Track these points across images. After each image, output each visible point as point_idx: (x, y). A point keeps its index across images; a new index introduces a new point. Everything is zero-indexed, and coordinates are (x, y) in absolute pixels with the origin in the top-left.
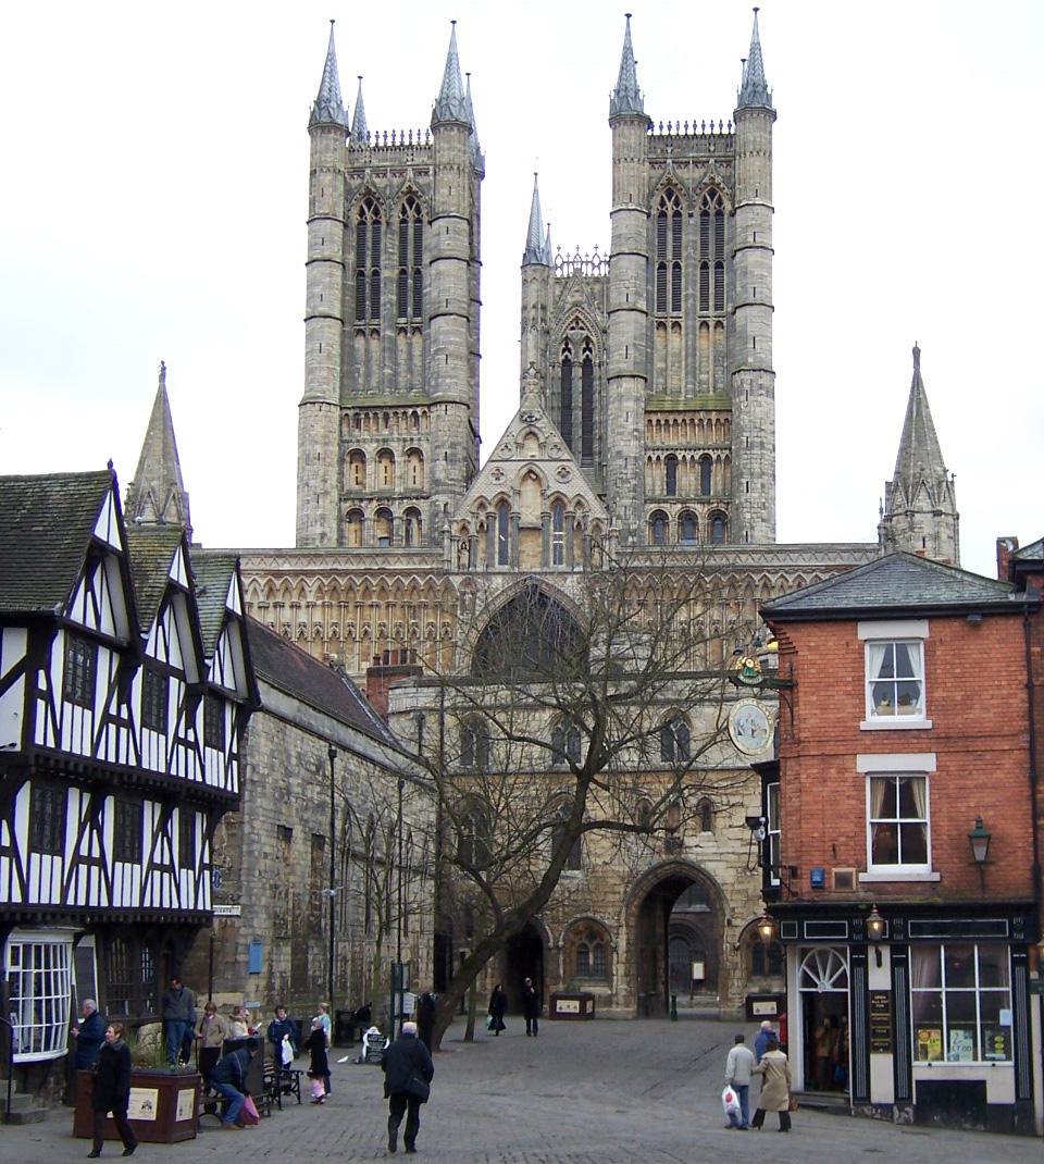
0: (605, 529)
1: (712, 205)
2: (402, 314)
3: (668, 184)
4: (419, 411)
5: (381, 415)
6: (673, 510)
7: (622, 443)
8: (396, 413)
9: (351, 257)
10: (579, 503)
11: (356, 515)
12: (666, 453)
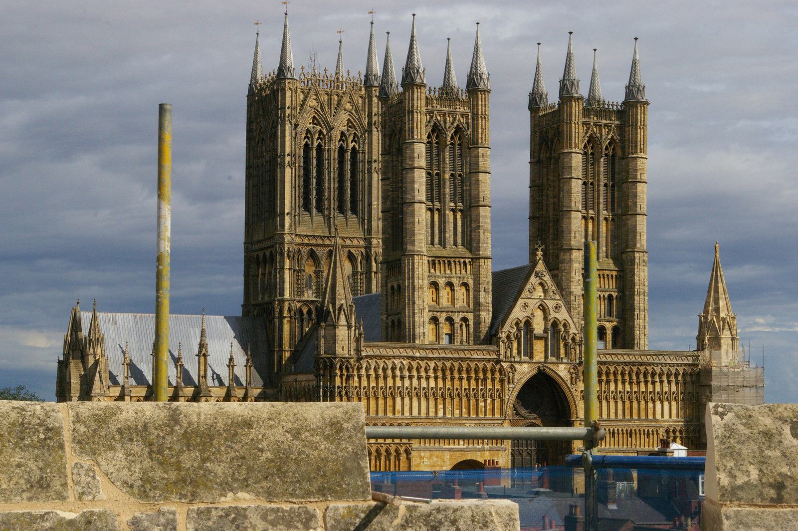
0: (578, 338)
4: (467, 260)
5: (446, 262)
8: (454, 261)
11: (435, 320)
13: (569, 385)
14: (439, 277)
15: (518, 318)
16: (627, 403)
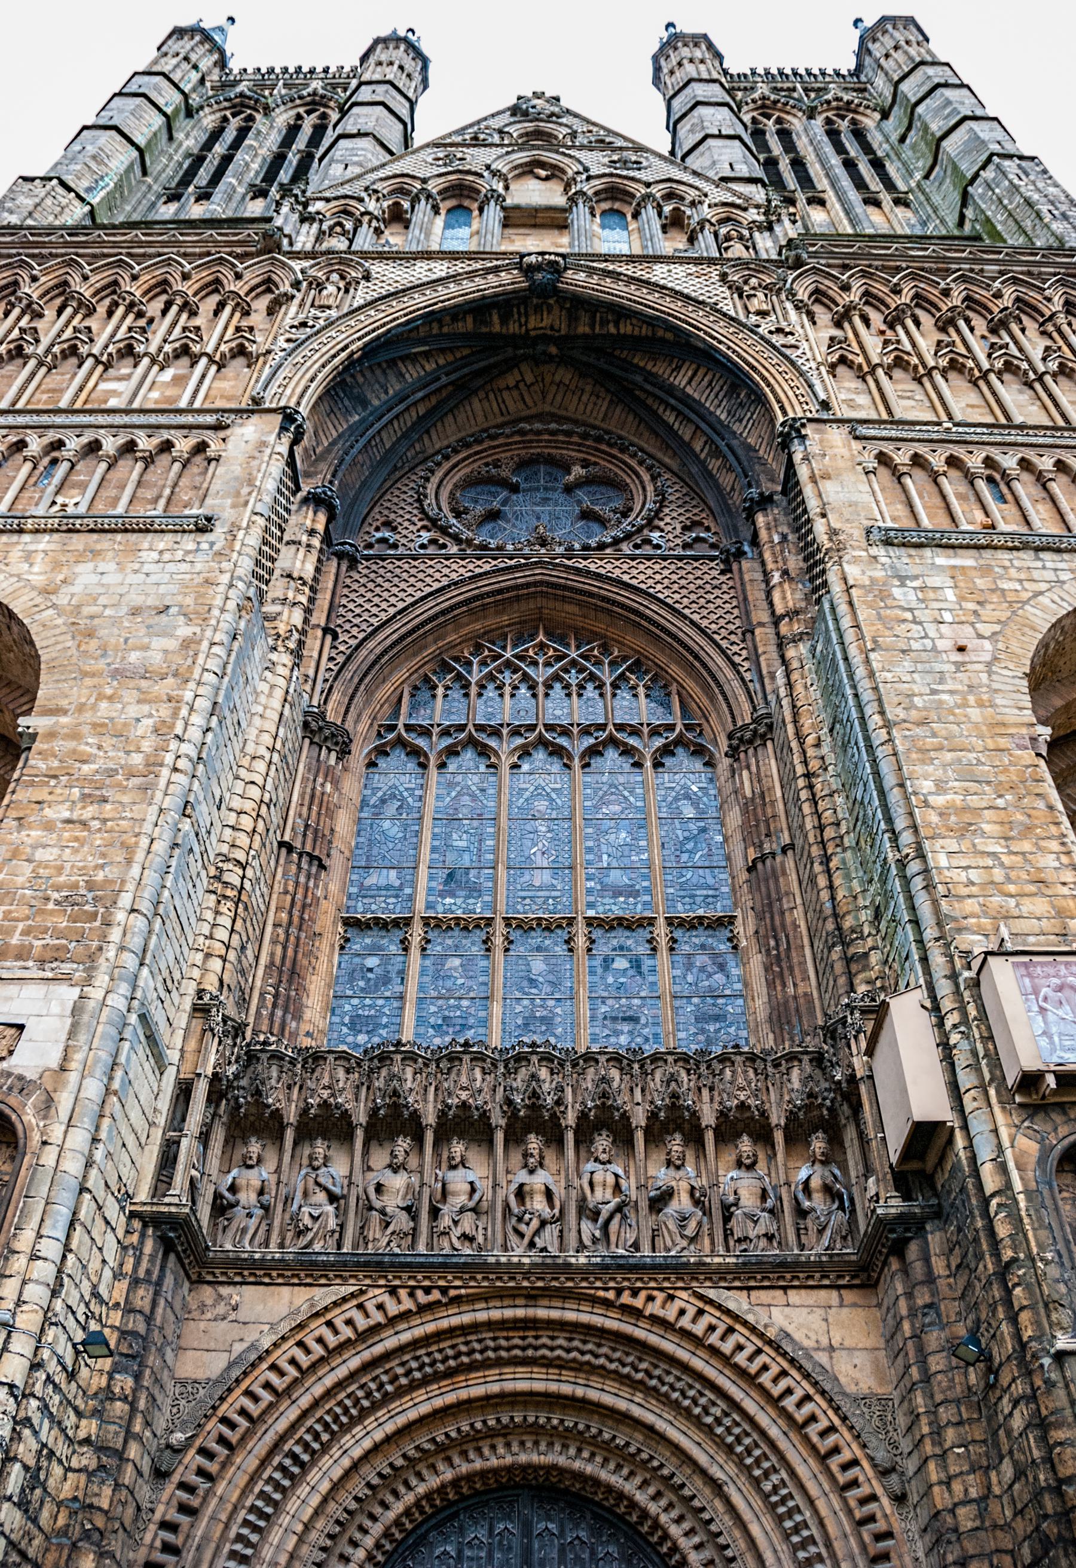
3: (763, 106)
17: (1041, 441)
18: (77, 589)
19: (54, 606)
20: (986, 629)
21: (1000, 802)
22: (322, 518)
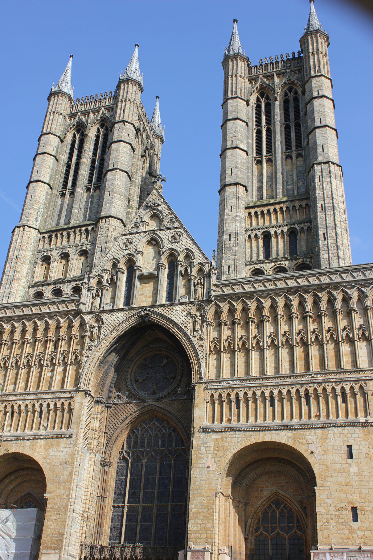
0: (207, 268)
1: (291, 96)
2: (90, 181)
5: (65, 233)
6: (268, 267)
7: (227, 225)
8: (74, 232)
9: (64, 158)
10: (187, 256)
12: (262, 231)
13: (189, 334)
14: (52, 250)
15: (114, 258)
16: (299, 351)
17: (251, 385)
18: (50, 457)
19: (47, 462)
20: (217, 459)
21: (205, 511)
22: (100, 407)
